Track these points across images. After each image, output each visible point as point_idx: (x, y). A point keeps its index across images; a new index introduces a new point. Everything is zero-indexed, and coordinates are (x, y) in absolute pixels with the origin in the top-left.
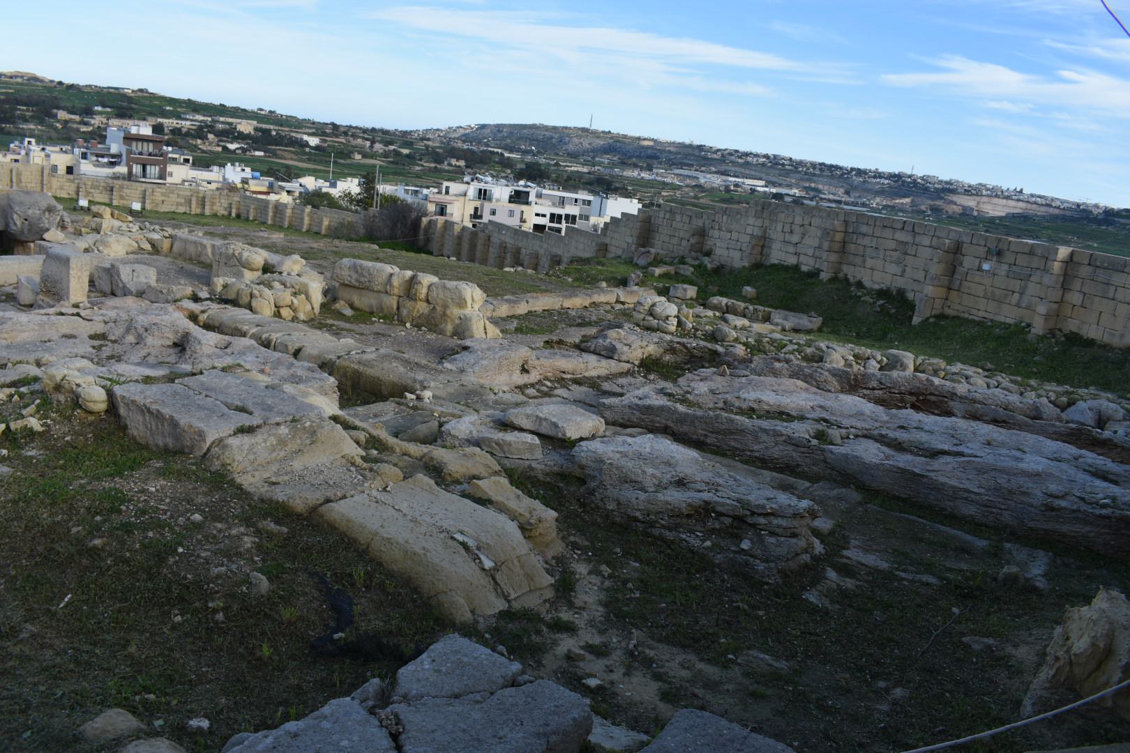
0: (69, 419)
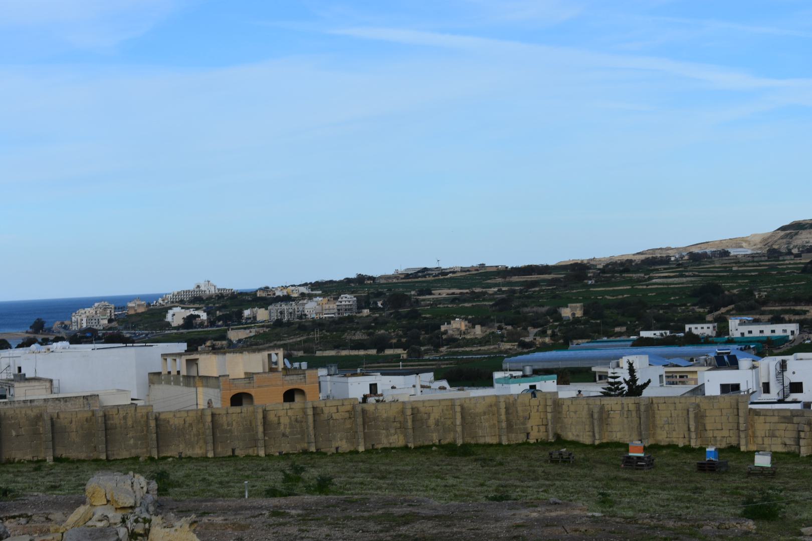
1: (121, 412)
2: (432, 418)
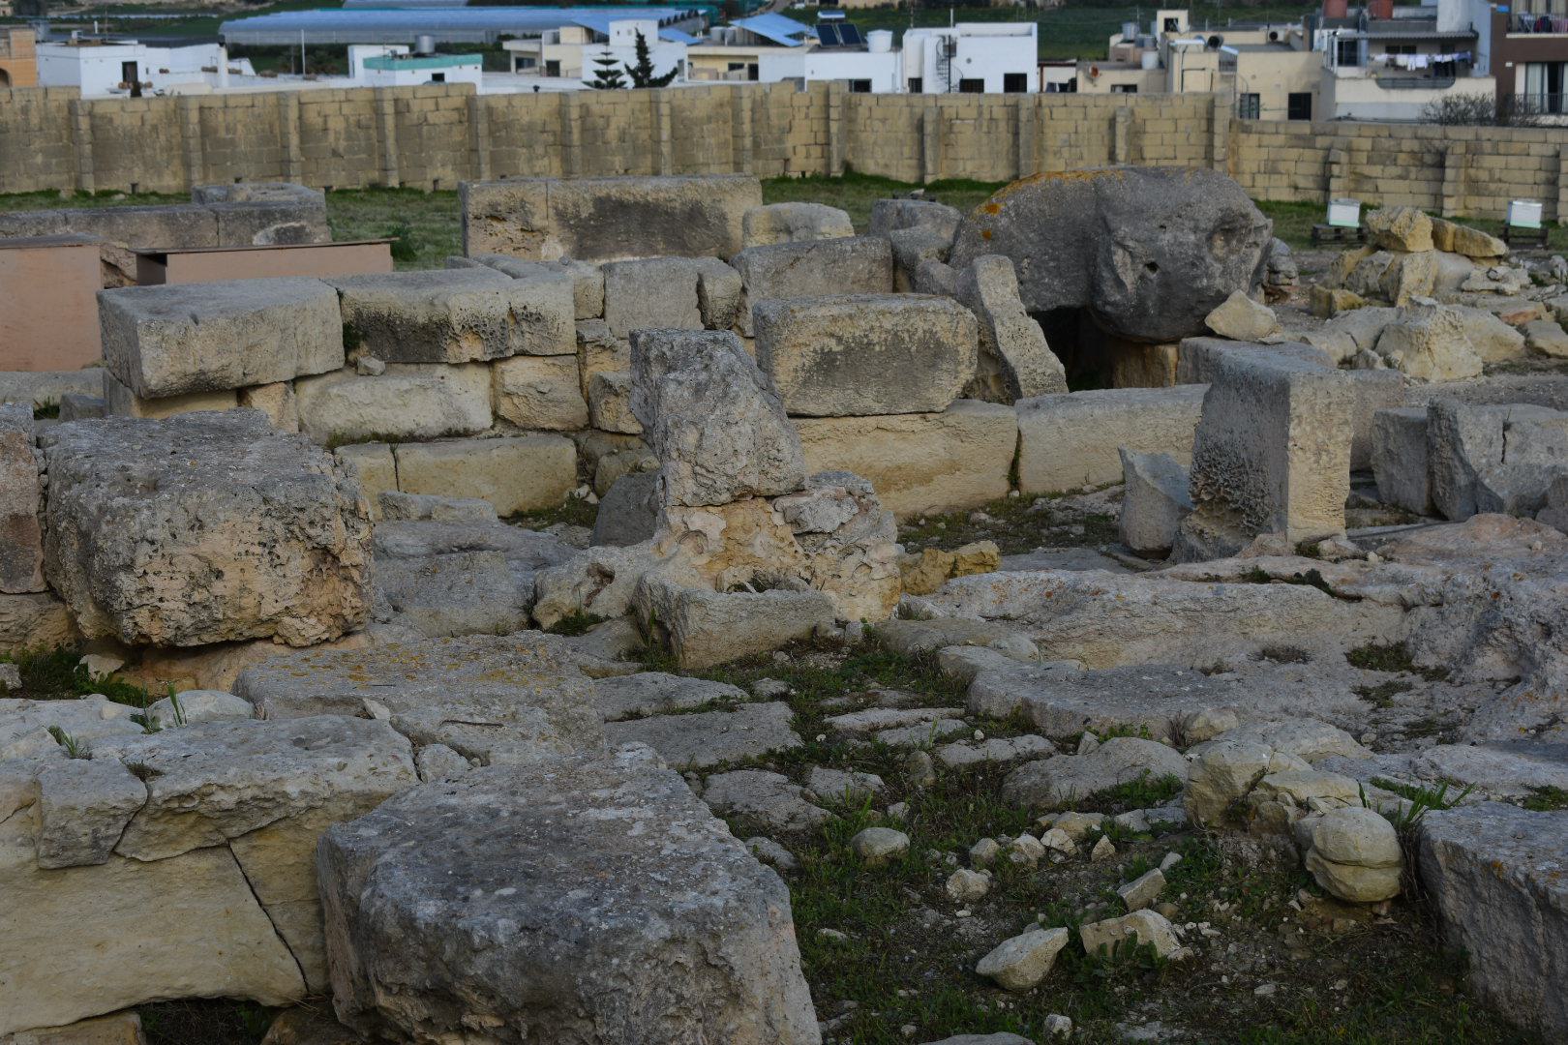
0: (1271, 921)
1: (17, 98)
2: (613, 126)
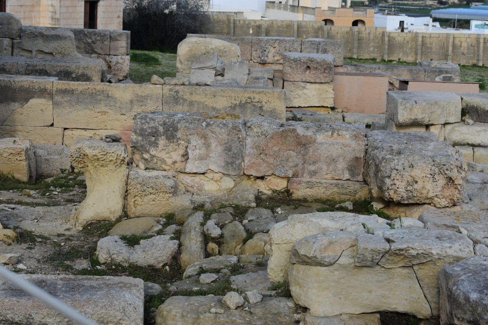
1: (367, 30)
